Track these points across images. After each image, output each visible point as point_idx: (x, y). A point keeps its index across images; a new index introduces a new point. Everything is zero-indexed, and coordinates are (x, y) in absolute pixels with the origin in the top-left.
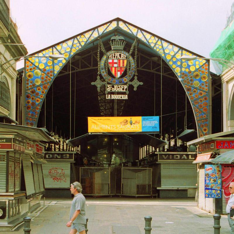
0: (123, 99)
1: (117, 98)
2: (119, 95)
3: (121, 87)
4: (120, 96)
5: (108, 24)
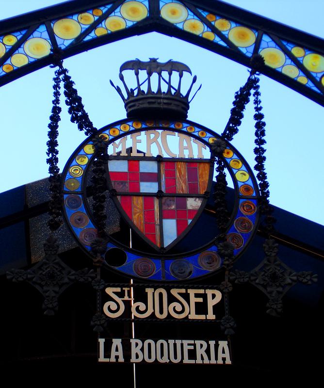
0: (206, 361)
1: (165, 360)
2: (178, 342)
3: (186, 297)
4: (186, 348)
5: (104, 10)
